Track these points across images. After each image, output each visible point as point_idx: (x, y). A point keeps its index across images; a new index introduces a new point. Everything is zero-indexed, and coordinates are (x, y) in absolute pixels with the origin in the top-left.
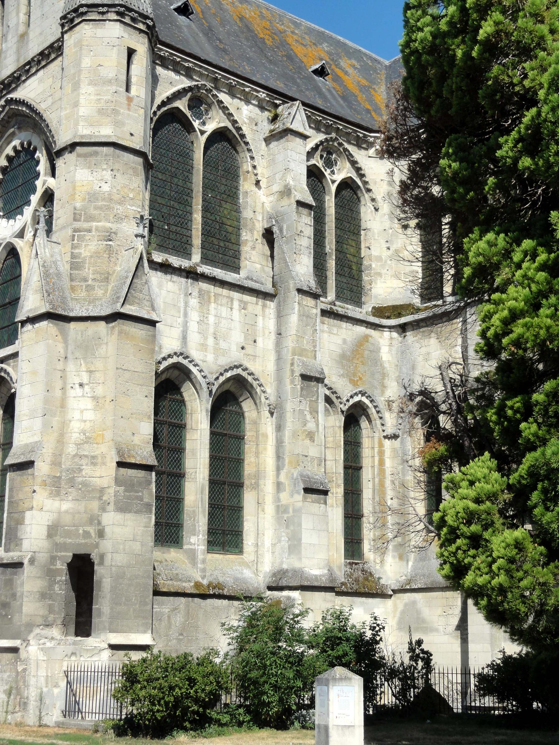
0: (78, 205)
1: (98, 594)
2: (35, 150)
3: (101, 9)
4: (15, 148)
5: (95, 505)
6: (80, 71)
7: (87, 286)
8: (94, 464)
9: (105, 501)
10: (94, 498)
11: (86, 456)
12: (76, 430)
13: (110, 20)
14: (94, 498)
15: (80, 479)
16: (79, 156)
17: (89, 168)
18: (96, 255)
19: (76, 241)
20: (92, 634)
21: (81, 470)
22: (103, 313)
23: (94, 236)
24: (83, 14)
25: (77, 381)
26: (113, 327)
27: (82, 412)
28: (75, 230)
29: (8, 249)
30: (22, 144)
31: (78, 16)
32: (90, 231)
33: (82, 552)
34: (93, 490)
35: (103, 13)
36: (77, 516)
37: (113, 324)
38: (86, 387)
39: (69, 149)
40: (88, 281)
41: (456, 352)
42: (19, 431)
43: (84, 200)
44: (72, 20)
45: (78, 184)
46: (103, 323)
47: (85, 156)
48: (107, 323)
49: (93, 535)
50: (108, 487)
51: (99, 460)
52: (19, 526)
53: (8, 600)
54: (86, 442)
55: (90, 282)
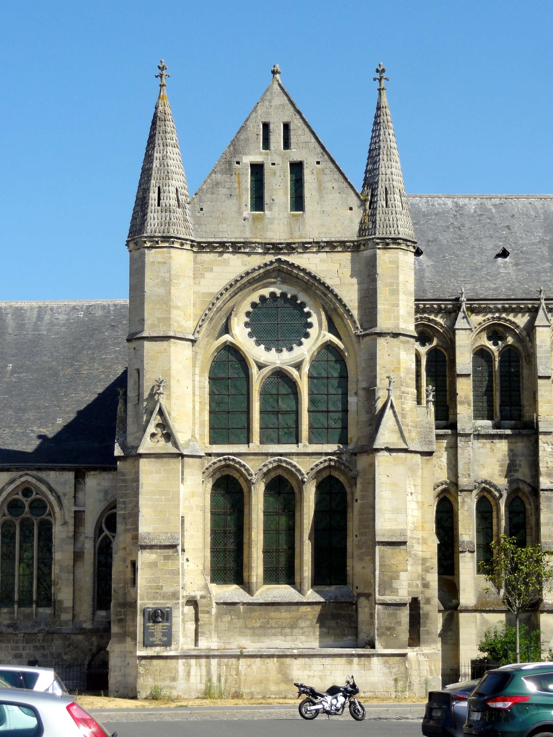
0: (402, 375)
1: (425, 622)
2: (303, 305)
3: (409, 243)
4: (273, 294)
5: (420, 568)
6: (398, 284)
7: (409, 430)
8: (418, 543)
9: (428, 567)
10: (419, 564)
11: (415, 538)
12: (410, 522)
13: (410, 251)
14: (419, 564)
15: (413, 552)
16: (401, 342)
17: (406, 351)
18: (411, 410)
19: (403, 400)
20: (421, 644)
21: (413, 546)
22: (420, 450)
23: (410, 397)
24: (399, 244)
25: (410, 491)
26: (428, 460)
27: (412, 511)
28: (403, 393)
29: (274, 371)
30: (284, 295)
31: (393, 243)
32: (408, 394)
33: (415, 597)
34: (419, 559)
35: (408, 246)
36: (413, 574)
37: (428, 457)
38: (413, 495)
39: (391, 335)
40: (408, 427)
41: (441, 461)
42: (382, 520)
43: (404, 372)
44: (388, 244)
45: (401, 361)
46: (419, 455)
47: (405, 342)
48: (421, 455)
49: (420, 586)
50: (431, 558)
51: (421, 541)
52: (393, 581)
53: (392, 625)
54: (415, 529)
55: (410, 428)
